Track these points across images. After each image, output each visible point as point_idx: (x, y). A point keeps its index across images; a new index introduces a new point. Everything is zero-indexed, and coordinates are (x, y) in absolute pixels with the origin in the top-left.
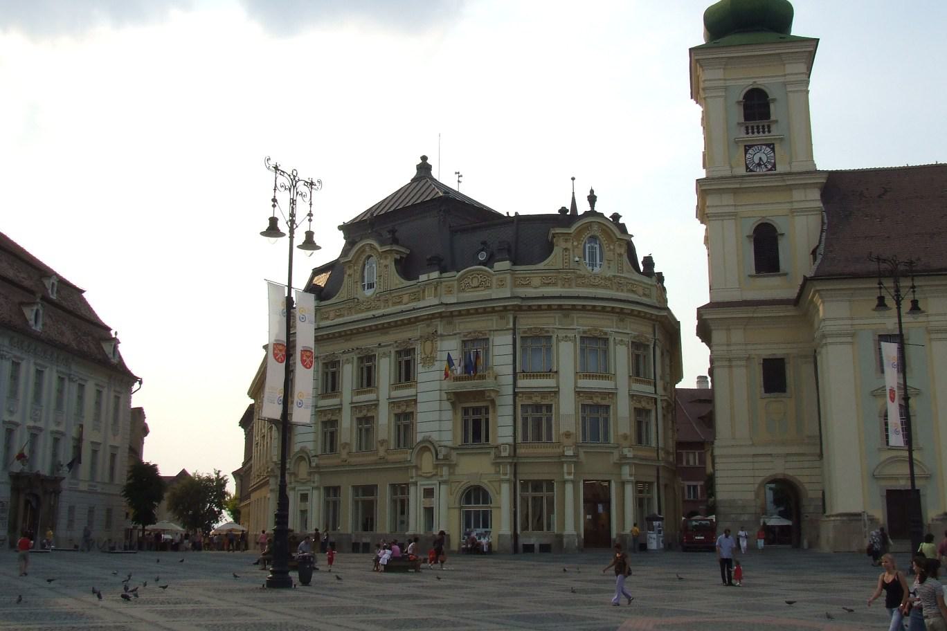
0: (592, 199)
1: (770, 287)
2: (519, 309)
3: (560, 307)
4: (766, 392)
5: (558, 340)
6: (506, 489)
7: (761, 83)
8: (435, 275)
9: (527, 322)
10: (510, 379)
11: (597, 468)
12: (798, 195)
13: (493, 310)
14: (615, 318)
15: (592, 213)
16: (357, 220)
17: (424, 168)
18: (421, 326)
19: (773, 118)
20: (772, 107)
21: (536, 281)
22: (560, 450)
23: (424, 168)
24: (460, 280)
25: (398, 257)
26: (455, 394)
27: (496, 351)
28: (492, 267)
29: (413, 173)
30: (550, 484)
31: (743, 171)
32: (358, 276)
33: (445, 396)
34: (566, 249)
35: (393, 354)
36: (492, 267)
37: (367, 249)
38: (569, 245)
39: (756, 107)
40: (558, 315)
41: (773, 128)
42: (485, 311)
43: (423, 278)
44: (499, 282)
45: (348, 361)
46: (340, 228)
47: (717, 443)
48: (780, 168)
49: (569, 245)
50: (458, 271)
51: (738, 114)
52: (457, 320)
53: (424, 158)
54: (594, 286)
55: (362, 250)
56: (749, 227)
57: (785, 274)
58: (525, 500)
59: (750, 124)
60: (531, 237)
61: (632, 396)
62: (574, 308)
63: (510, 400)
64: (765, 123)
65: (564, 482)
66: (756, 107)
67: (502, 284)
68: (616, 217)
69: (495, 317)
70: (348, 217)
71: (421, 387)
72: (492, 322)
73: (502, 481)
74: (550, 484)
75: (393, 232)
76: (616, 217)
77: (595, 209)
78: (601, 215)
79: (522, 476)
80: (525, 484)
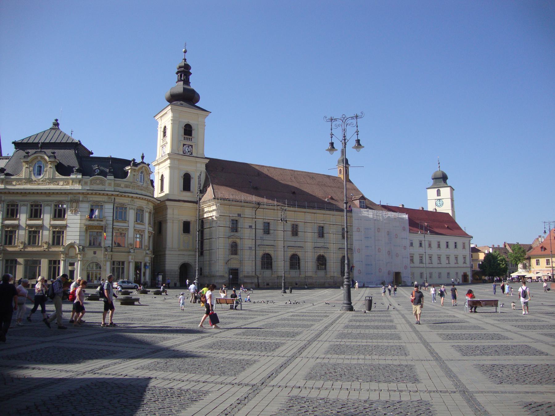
0: (143, 157)
1: (186, 196)
2: (118, 195)
3: (132, 197)
4: (184, 232)
5: (130, 209)
6: (108, 264)
7: (191, 122)
8: (80, 176)
9: (119, 200)
10: (111, 222)
11: (139, 258)
12: (199, 165)
13: (107, 195)
14: (146, 202)
15: (143, 163)
16: (25, 141)
17: (56, 124)
18: (70, 196)
19: (193, 135)
20: (193, 132)
21: (123, 185)
22: (128, 250)
23: (56, 124)
24: (91, 181)
25: (56, 164)
26: (89, 226)
27: (106, 210)
28: (106, 177)
29: (51, 126)
30: (123, 263)
31: (182, 153)
32: (31, 168)
33: (83, 226)
34: (134, 175)
35: (53, 206)
36: (106, 177)
37: (39, 158)
38: (135, 173)
39: (188, 130)
40: (130, 199)
41: (193, 139)
42: (103, 194)
43: (73, 176)
44: (110, 183)
45: (24, 205)
46: (13, 143)
47: (167, 249)
48: (194, 154)
49: (135, 173)
50: (91, 176)
51: (182, 132)
52: (89, 196)
53: (57, 120)
54: (141, 190)
55: (37, 158)
56: (182, 174)
57: (192, 192)
58: (113, 268)
59: (186, 136)
60: (117, 167)
61: (149, 232)
62: (137, 198)
63: (111, 230)
64: (191, 137)
65: (129, 262)
66: (188, 130)
67: (110, 184)
68: (148, 165)
69: (106, 197)
70: (18, 139)
71: (69, 221)
72: (105, 198)
73: (107, 261)
74: (123, 263)
75: (54, 153)
76: (148, 165)
77: (144, 161)
78: (145, 163)
79: (113, 260)
80: (114, 262)
